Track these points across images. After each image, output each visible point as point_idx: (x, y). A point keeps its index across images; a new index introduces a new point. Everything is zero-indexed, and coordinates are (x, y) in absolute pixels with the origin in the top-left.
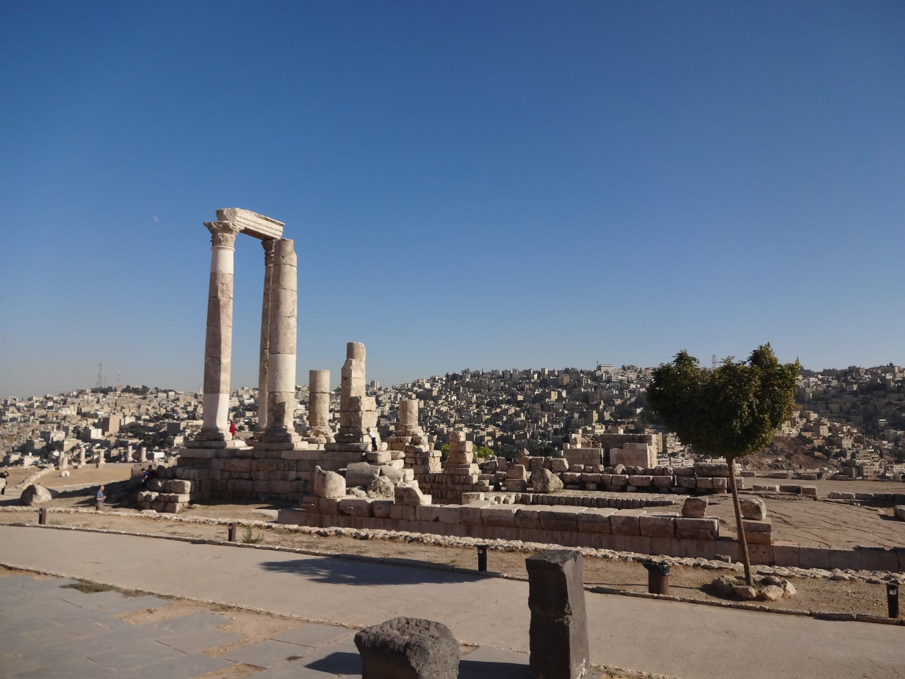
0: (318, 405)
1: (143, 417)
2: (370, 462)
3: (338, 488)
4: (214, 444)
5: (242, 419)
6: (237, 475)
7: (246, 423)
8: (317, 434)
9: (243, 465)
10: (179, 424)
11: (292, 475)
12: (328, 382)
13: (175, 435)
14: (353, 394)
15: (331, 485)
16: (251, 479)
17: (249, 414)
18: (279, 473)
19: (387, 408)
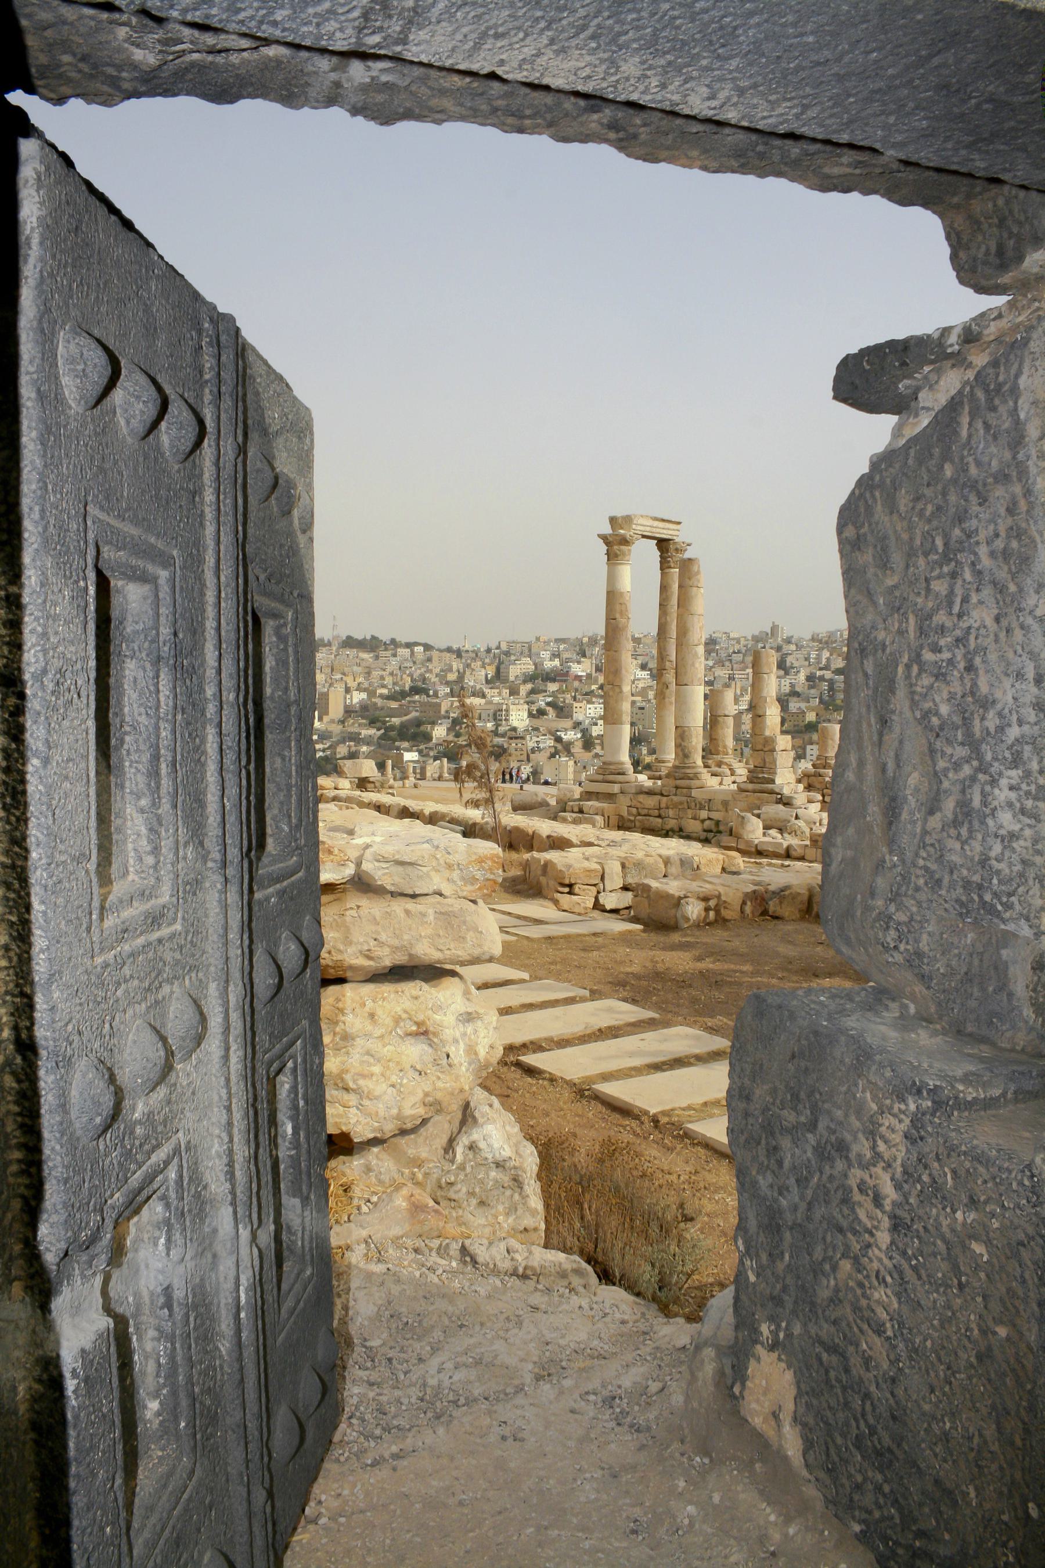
0: (720, 732)
1: (379, 691)
2: (785, 804)
3: (755, 831)
4: (620, 778)
5: (540, 697)
6: (645, 812)
7: (548, 704)
8: (719, 764)
9: (651, 802)
10: (439, 705)
11: (704, 814)
12: (731, 705)
13: (433, 723)
14: (767, 733)
15: (749, 827)
16: (659, 816)
17: (552, 687)
18: (689, 812)
19: (802, 677)
